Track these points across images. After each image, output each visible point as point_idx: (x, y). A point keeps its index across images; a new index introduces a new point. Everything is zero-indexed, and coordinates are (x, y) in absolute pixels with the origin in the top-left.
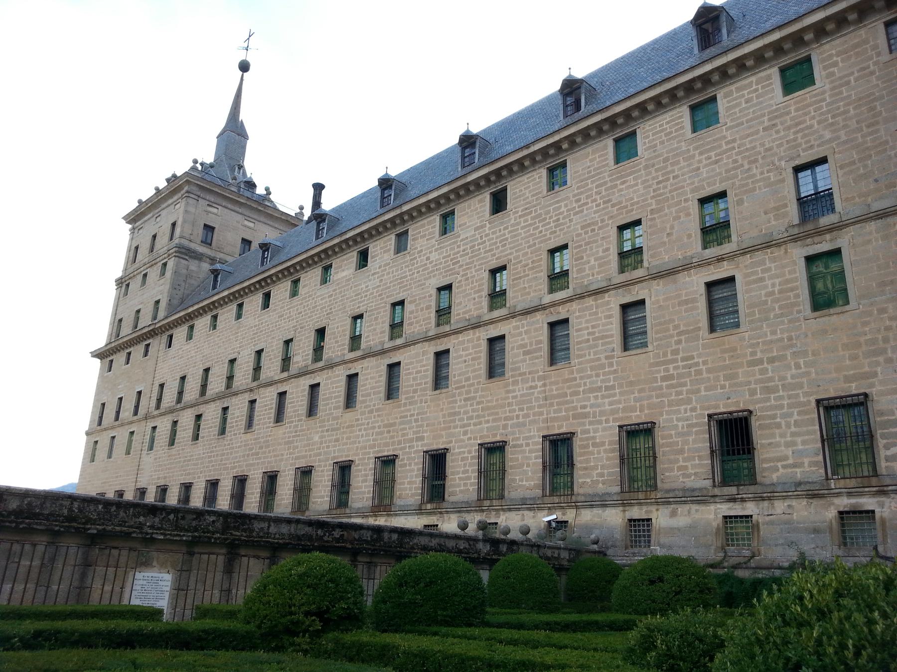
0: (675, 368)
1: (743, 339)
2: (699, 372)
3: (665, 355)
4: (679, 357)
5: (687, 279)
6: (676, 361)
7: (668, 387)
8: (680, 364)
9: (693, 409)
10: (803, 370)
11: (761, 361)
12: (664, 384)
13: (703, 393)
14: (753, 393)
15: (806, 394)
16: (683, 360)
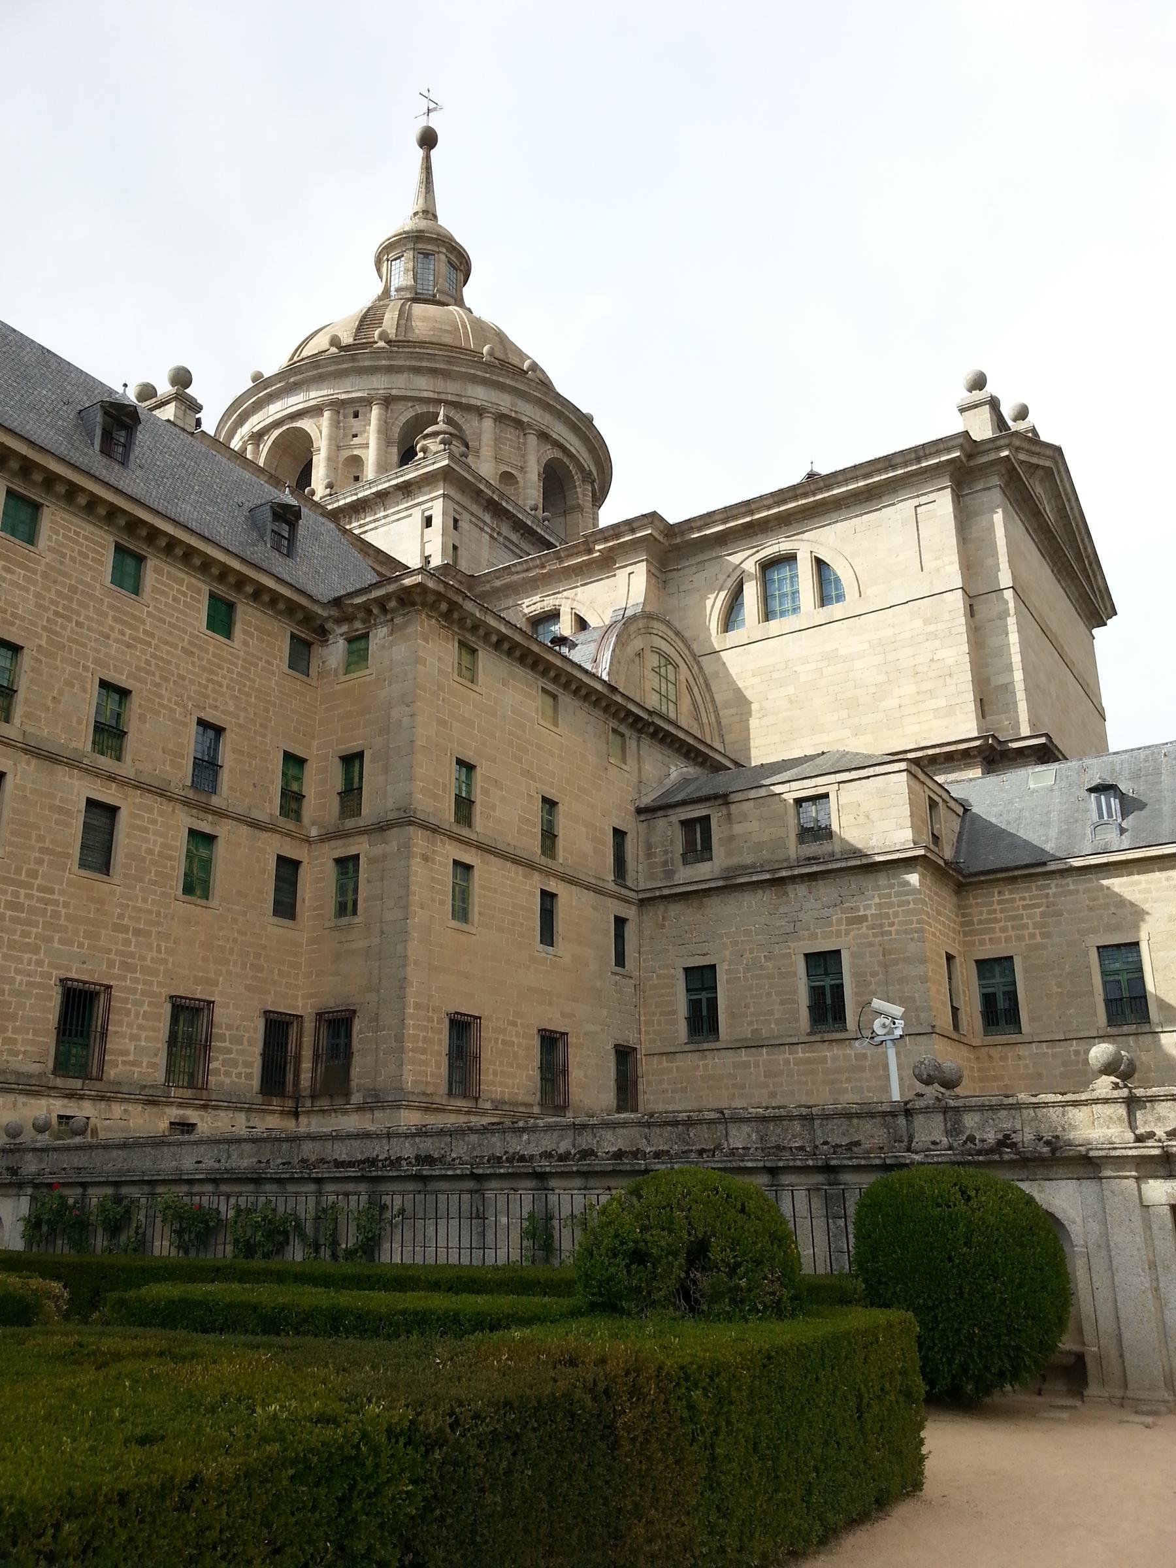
0: (27, 896)
1: (113, 893)
2: (56, 915)
3: (18, 871)
4: (37, 882)
5: (67, 779)
6: (29, 886)
7: (13, 920)
8: (35, 893)
9: (40, 963)
10: (163, 956)
11: (125, 929)
12: (9, 913)
13: (56, 945)
14: (111, 964)
15: (160, 984)
16: (41, 889)
